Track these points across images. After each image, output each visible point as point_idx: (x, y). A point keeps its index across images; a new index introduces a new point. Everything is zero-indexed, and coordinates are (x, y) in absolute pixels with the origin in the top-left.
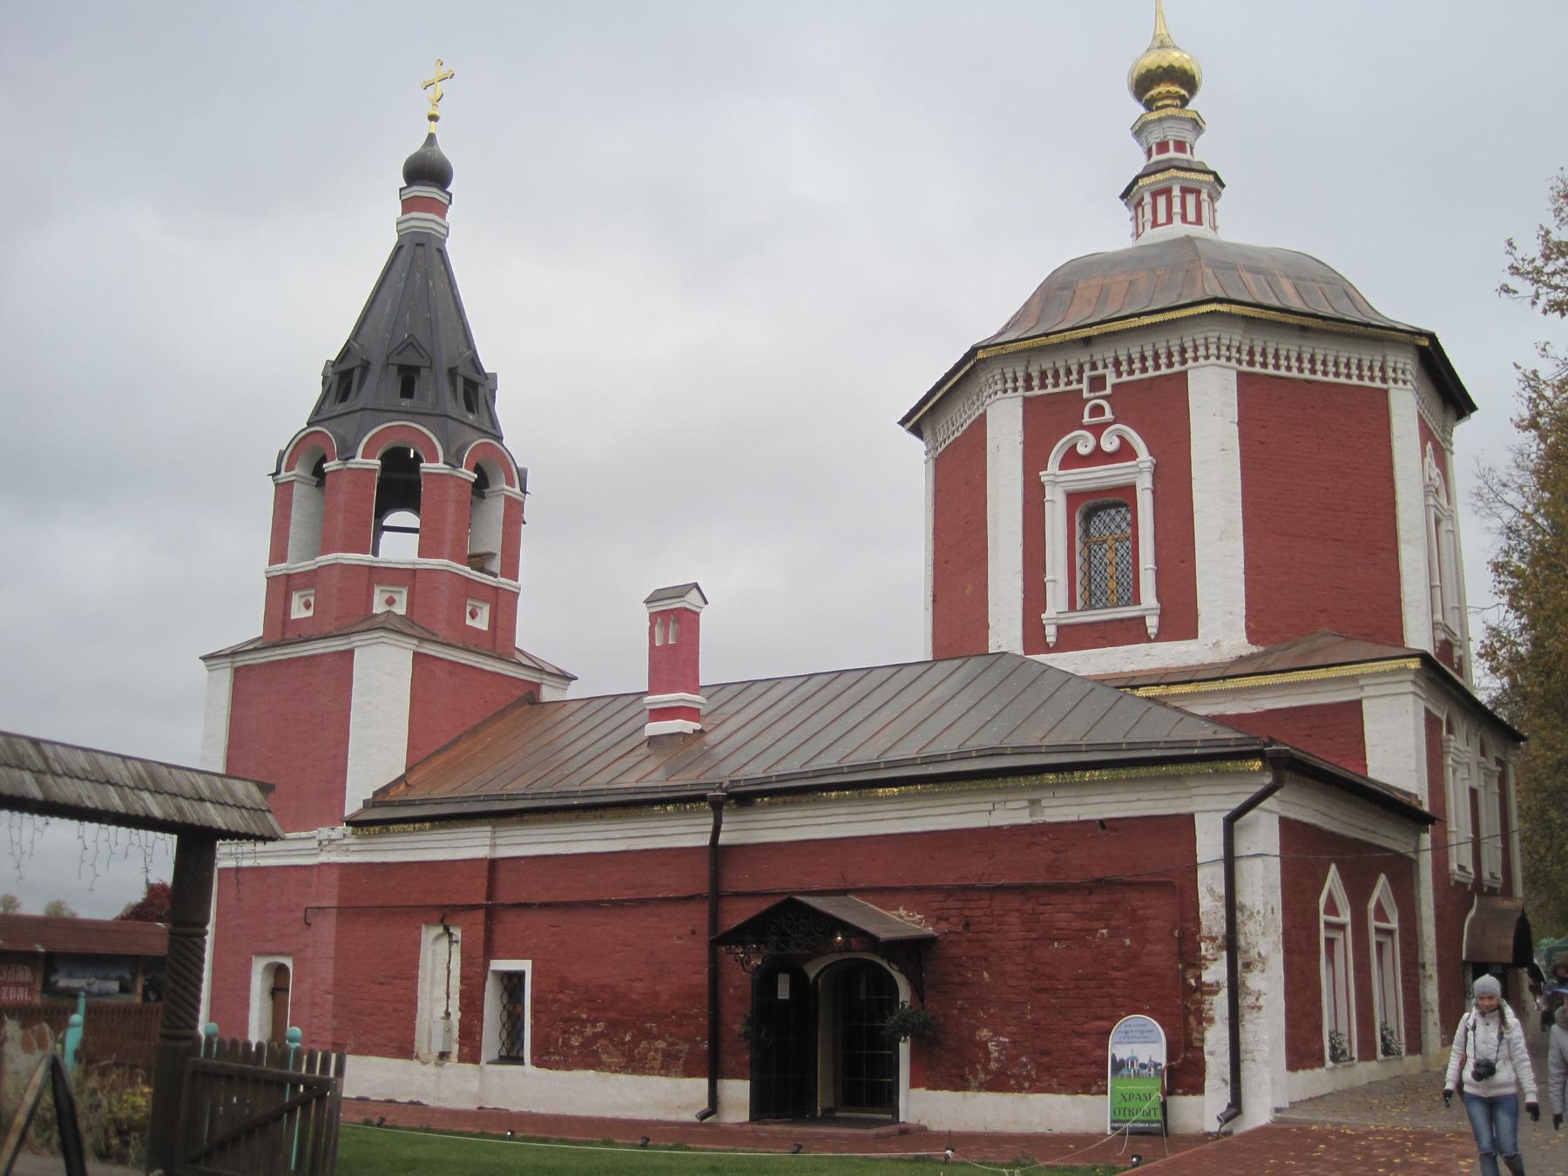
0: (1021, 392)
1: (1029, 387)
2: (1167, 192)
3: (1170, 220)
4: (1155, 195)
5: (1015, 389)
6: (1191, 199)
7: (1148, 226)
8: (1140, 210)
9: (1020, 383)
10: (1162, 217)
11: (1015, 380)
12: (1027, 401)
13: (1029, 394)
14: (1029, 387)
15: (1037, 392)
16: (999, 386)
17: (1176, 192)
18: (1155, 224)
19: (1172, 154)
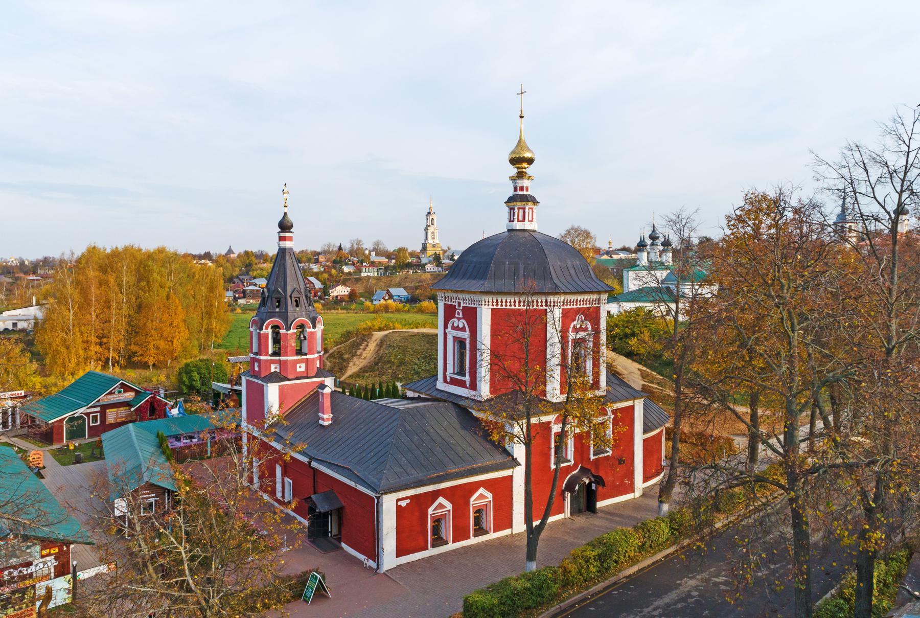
0: (491, 307)
1: (493, 305)
2: (524, 209)
3: (524, 220)
4: (519, 209)
5: (488, 305)
6: (530, 210)
7: (516, 220)
8: (512, 211)
9: (491, 303)
10: (521, 218)
11: (488, 302)
12: (492, 309)
13: (493, 307)
14: (493, 305)
15: (495, 307)
16: (483, 303)
17: (527, 211)
18: (518, 221)
19: (525, 193)
